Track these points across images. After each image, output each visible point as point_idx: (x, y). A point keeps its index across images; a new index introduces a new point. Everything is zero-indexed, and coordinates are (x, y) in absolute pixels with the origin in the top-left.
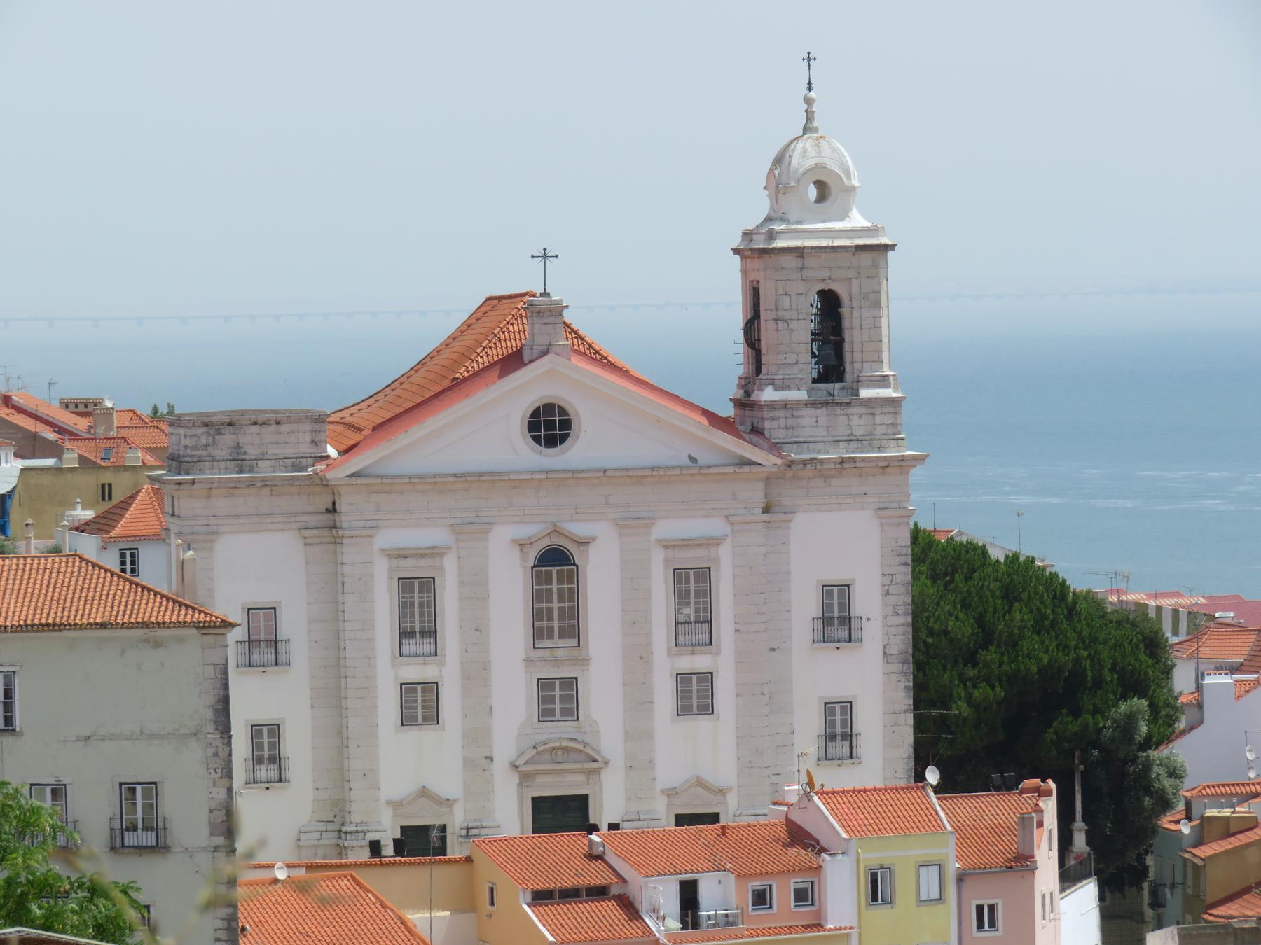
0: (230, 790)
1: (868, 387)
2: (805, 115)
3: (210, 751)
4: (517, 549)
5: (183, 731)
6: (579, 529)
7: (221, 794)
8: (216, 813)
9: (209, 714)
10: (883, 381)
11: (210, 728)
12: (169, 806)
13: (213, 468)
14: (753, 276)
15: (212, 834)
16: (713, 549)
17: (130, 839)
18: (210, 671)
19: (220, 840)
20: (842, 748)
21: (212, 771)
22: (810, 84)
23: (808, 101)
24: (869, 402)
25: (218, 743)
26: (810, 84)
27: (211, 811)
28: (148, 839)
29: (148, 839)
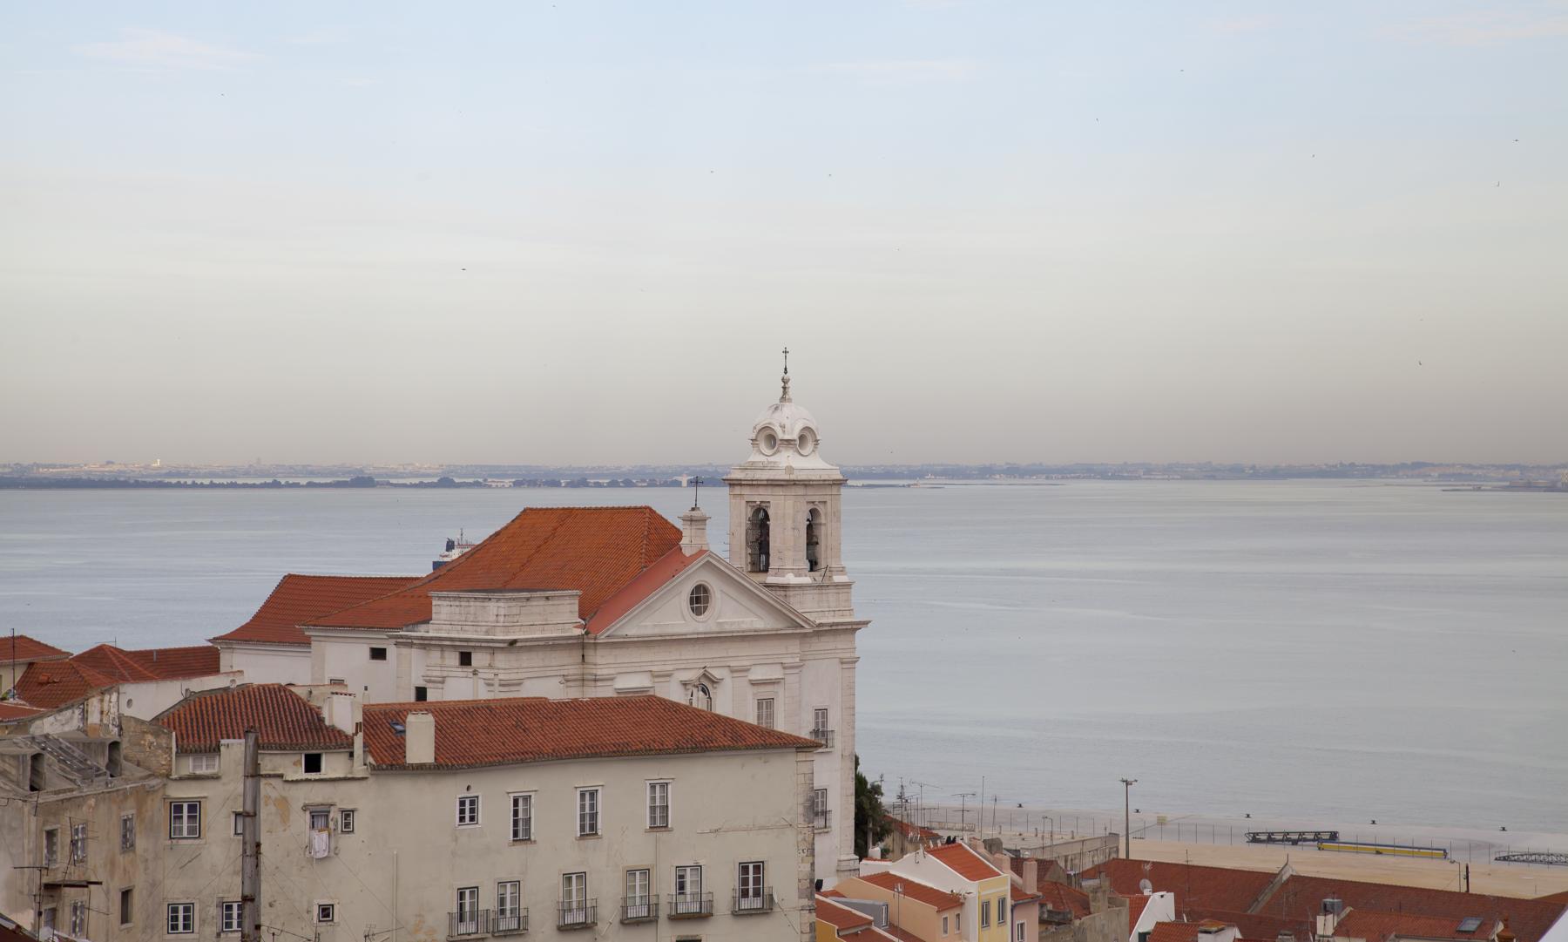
0: (813, 864)
1: (837, 575)
2: (782, 389)
3: (800, 837)
4: (682, 687)
5: (784, 823)
6: (716, 673)
7: (807, 867)
8: (802, 881)
9: (801, 809)
10: (842, 571)
11: (801, 819)
12: (773, 880)
13: (520, 631)
14: (758, 500)
15: (800, 898)
16: (776, 686)
17: (745, 904)
18: (801, 779)
19: (805, 902)
20: (819, 822)
21: (801, 851)
22: (786, 369)
23: (785, 381)
24: (837, 585)
25: (806, 831)
26: (786, 369)
27: (799, 881)
28: (757, 903)
29: (757, 903)
